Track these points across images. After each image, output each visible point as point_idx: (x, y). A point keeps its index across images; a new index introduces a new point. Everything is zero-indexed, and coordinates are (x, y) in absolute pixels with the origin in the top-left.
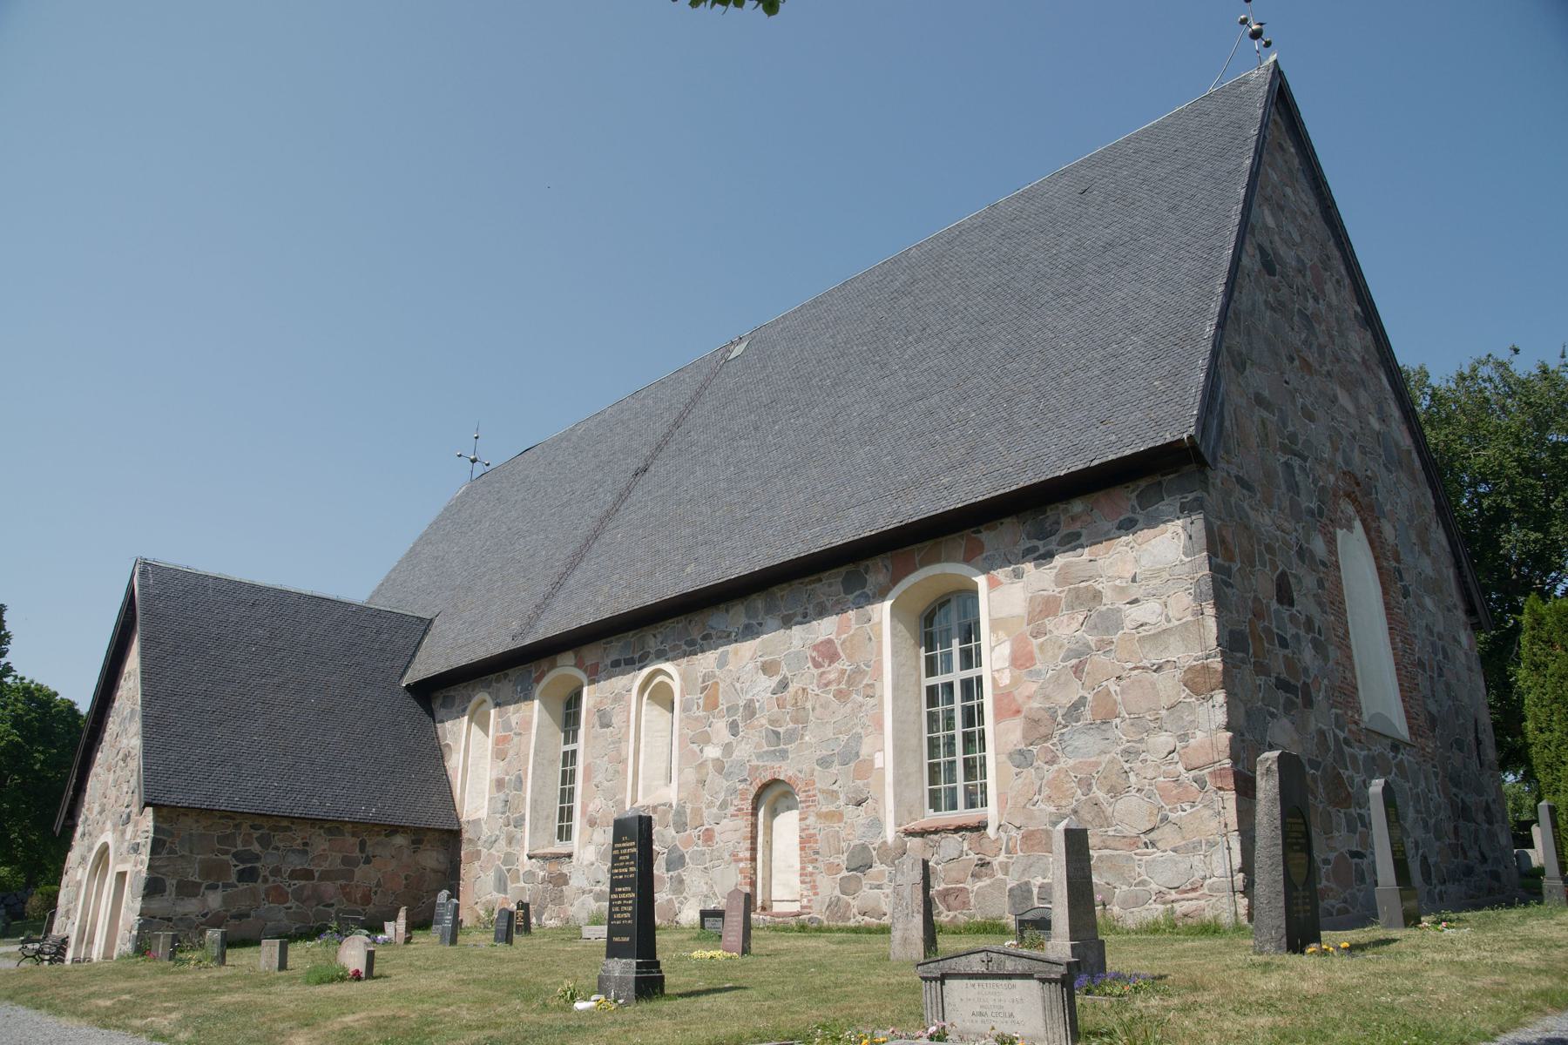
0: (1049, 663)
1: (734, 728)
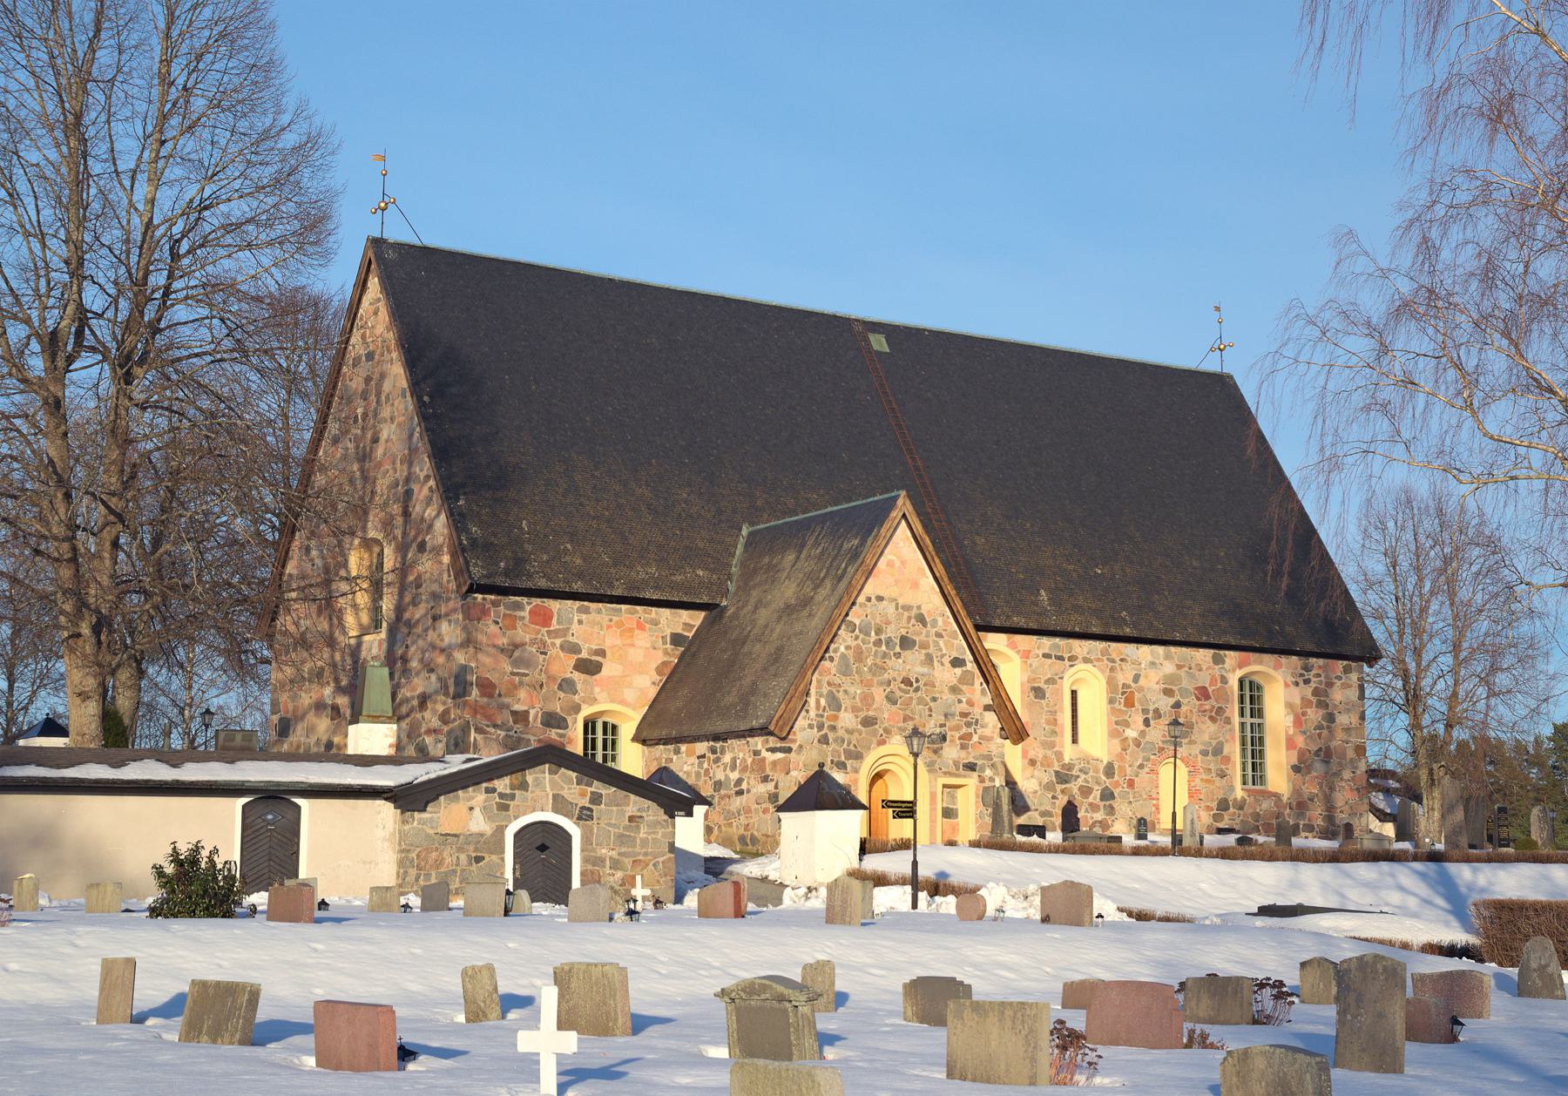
1: (1147, 723)
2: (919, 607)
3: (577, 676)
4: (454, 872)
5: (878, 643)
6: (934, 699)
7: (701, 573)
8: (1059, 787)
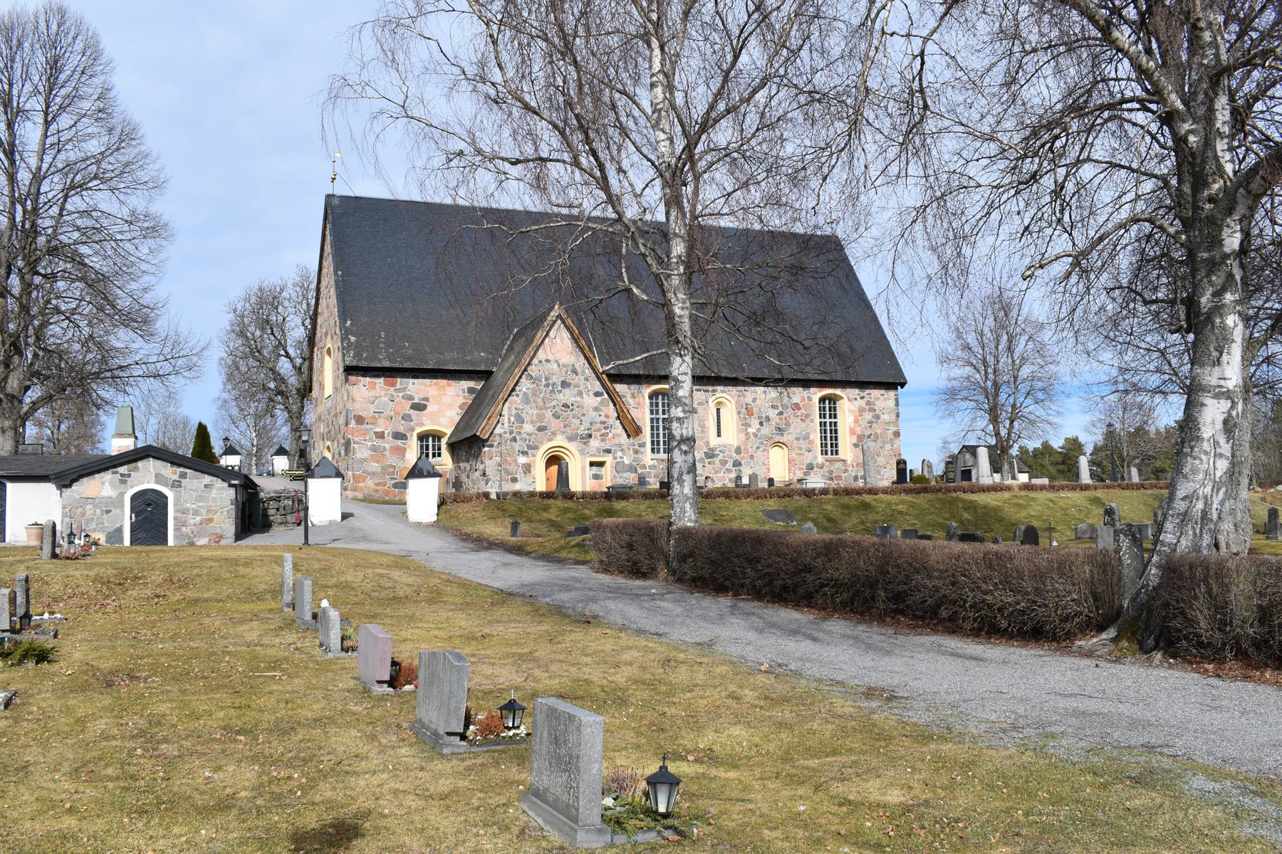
0: (864, 424)
1: (761, 424)
2: (573, 365)
3: (412, 412)
4: (93, 519)
5: (547, 385)
6: (584, 415)
7: (482, 354)
8: (707, 461)
